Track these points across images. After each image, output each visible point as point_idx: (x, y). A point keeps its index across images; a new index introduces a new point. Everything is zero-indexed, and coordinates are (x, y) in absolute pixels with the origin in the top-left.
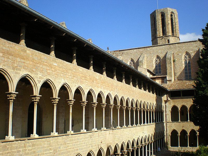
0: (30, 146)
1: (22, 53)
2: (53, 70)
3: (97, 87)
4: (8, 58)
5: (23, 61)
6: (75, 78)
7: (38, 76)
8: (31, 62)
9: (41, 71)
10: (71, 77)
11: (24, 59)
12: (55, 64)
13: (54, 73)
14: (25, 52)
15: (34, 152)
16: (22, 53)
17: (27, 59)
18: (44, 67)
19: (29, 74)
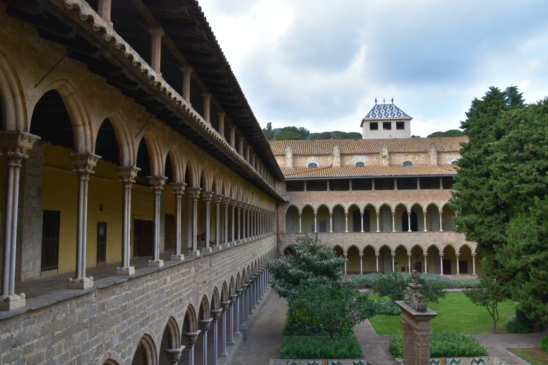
0: (358, 236)
1: (349, 194)
2: (373, 197)
3: (426, 200)
4: (342, 198)
5: (350, 197)
6: (395, 198)
7: (361, 203)
8: (356, 197)
9: (363, 200)
10: (390, 199)
11: (351, 197)
12: (374, 194)
13: (374, 199)
14: (352, 193)
15: (361, 239)
16: (349, 194)
17: (353, 196)
18: (365, 197)
19: (355, 203)
